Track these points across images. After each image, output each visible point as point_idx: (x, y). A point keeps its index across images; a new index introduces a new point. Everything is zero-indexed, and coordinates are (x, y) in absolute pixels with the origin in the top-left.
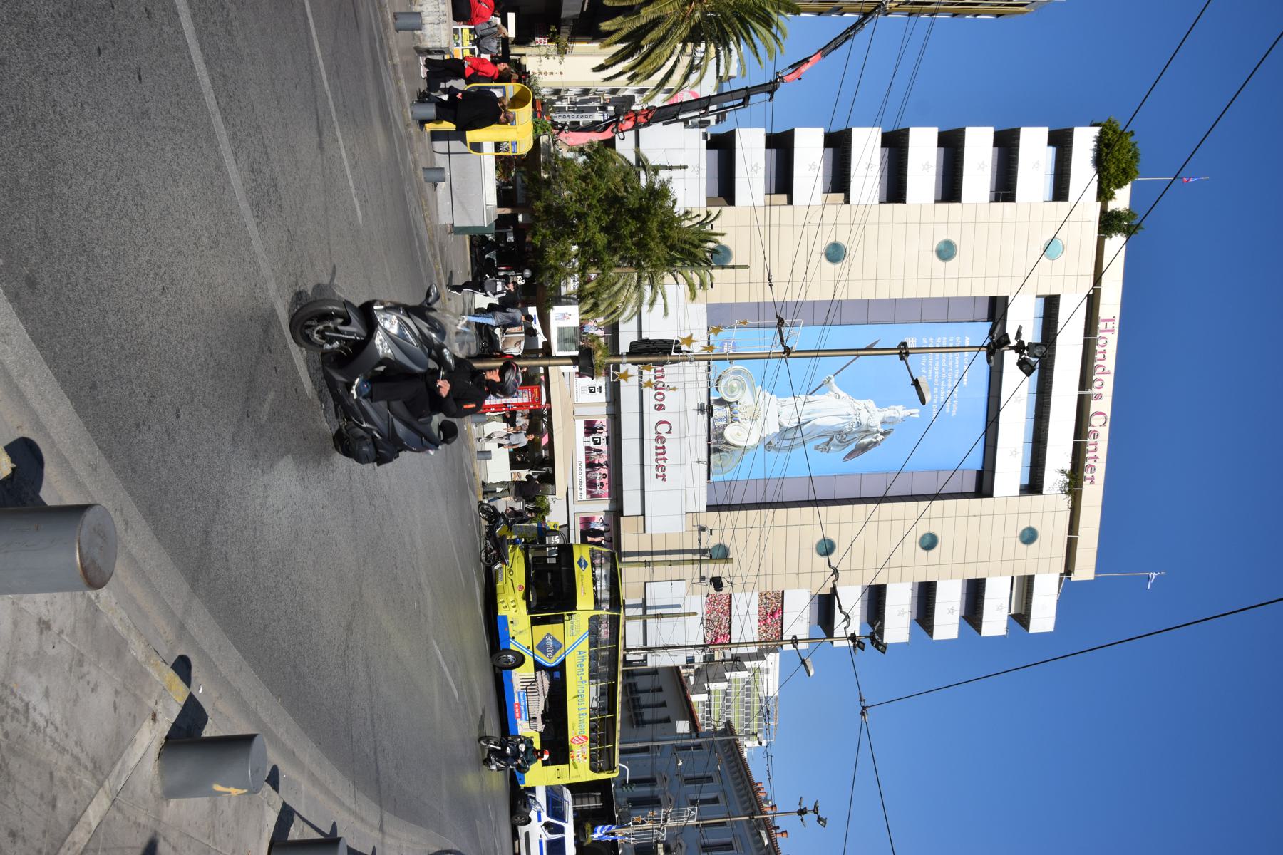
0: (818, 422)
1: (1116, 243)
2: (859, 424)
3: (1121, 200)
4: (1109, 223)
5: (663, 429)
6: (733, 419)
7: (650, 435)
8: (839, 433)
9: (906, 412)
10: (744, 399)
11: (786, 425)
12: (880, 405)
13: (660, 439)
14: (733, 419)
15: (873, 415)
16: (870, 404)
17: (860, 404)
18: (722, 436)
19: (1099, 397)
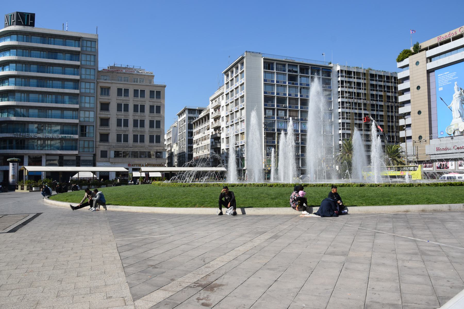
0: (459, 108)
1: (423, 45)
2: (459, 97)
3: (412, 49)
4: (417, 49)
5: (456, 148)
6: (458, 130)
7: (457, 151)
8: (461, 101)
9: (456, 85)
10: (453, 128)
11: (459, 116)
12: (454, 93)
13: (458, 148)
14: (458, 130)
15: (457, 93)
16: (454, 95)
17: (454, 98)
18: (462, 132)
19: (456, 32)
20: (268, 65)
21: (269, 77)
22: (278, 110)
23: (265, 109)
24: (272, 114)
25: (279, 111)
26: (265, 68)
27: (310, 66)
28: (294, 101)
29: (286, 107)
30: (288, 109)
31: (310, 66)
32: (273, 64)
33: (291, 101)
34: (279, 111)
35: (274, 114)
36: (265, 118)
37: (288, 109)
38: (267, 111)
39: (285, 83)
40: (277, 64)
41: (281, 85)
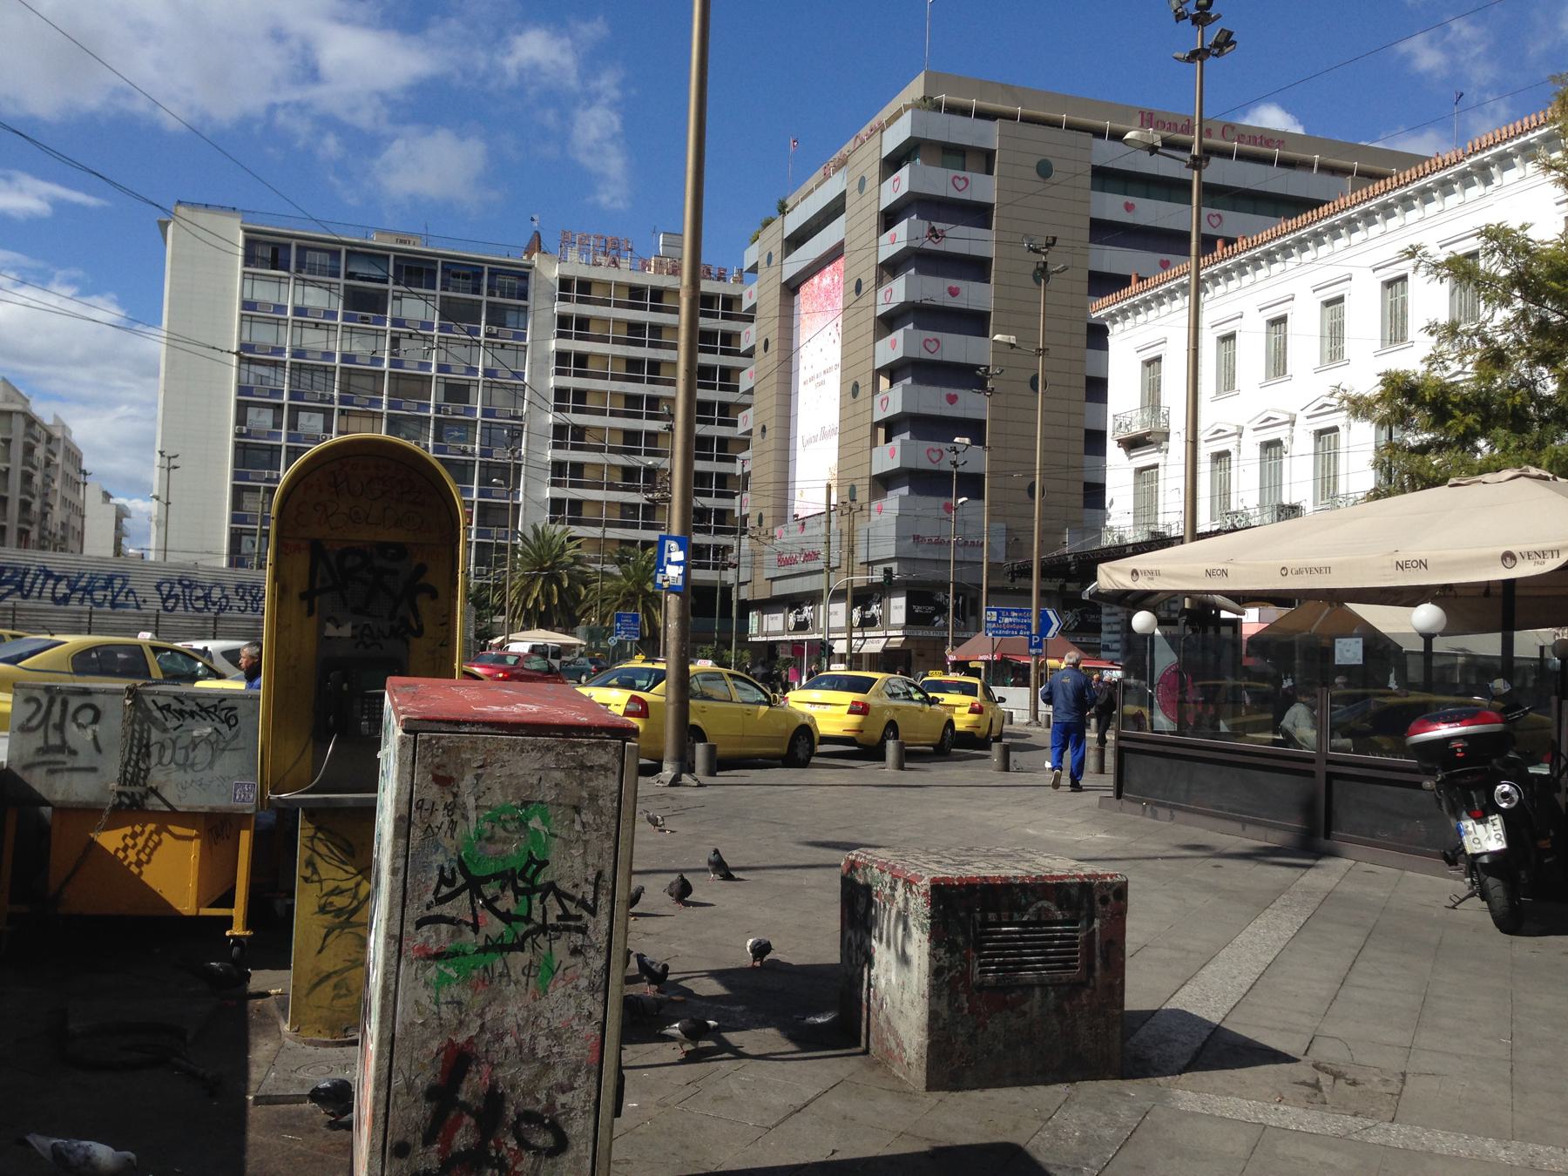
20: (267, 253)
21: (264, 293)
22: (295, 411)
23: (242, 407)
24: (269, 422)
25: (303, 417)
26: (249, 259)
27: (440, 260)
28: (368, 382)
29: (331, 401)
30: (337, 406)
31: (440, 260)
32: (288, 246)
33: (355, 380)
34: (303, 417)
35: (277, 425)
36: (238, 435)
37: (337, 406)
38: (252, 413)
39: (333, 315)
40: (299, 247)
41: (317, 325)
